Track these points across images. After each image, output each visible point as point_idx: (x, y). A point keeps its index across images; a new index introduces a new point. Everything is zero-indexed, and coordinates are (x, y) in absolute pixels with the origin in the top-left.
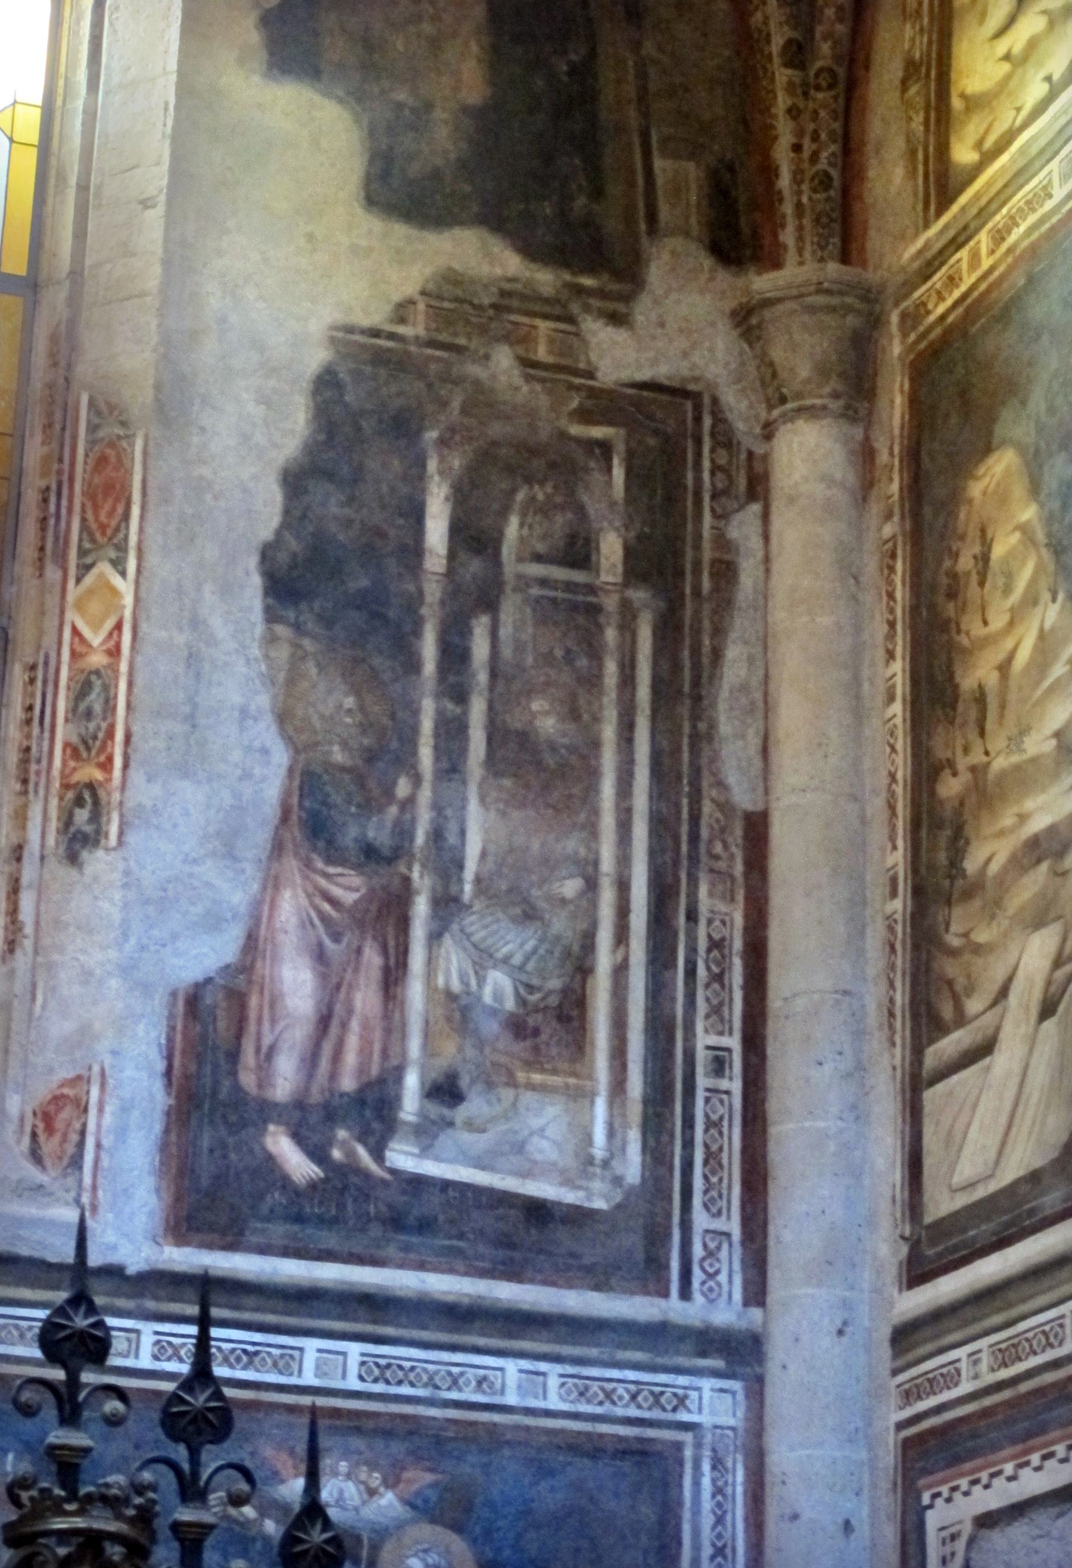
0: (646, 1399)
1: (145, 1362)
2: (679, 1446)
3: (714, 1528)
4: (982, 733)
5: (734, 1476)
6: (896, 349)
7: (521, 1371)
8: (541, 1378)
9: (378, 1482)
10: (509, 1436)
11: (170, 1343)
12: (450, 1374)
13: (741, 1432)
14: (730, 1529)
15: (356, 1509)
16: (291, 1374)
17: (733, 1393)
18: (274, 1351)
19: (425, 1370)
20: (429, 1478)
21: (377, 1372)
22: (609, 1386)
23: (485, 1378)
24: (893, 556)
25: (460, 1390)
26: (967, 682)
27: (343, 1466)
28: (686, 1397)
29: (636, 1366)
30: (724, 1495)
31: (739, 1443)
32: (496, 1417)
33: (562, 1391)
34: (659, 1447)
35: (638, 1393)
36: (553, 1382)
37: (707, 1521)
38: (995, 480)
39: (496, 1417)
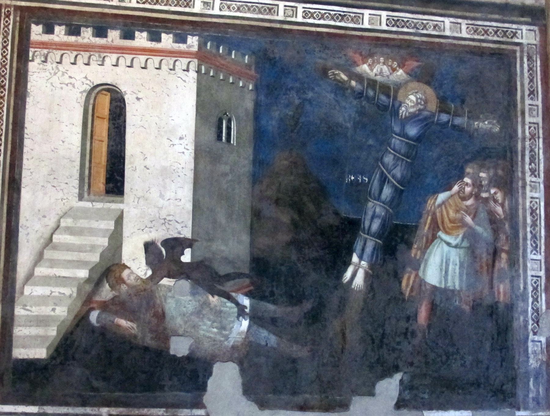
0: (501, 33)
1: (300, 19)
2: (515, 52)
3: (529, 84)
5: (536, 63)
7: (451, 22)
8: (459, 25)
9: (396, 66)
10: (447, 48)
11: (309, 12)
12: (423, 23)
13: (538, 46)
14: (535, 83)
15: (388, 76)
16: (359, 24)
17: (535, 31)
18: (351, 15)
19: (413, 22)
20: (416, 64)
21: (393, 23)
22: (486, 28)
23: (437, 25)
25: (427, 30)
27: (382, 59)
28: (516, 33)
29: (496, 21)
30: (533, 71)
31: (538, 50)
32: (442, 40)
33: (468, 30)
34: (506, 52)
35: (498, 30)
36: (464, 27)
37: (526, 81)
39: (442, 40)
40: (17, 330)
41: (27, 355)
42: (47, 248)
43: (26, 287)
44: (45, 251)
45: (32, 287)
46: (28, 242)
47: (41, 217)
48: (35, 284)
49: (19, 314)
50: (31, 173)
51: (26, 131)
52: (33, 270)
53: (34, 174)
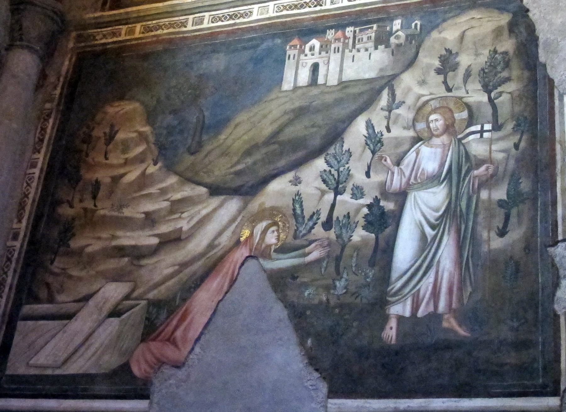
4: (94, 197)
6: (71, 45)
24: (49, 116)
26: (89, 176)
38: (124, 110)
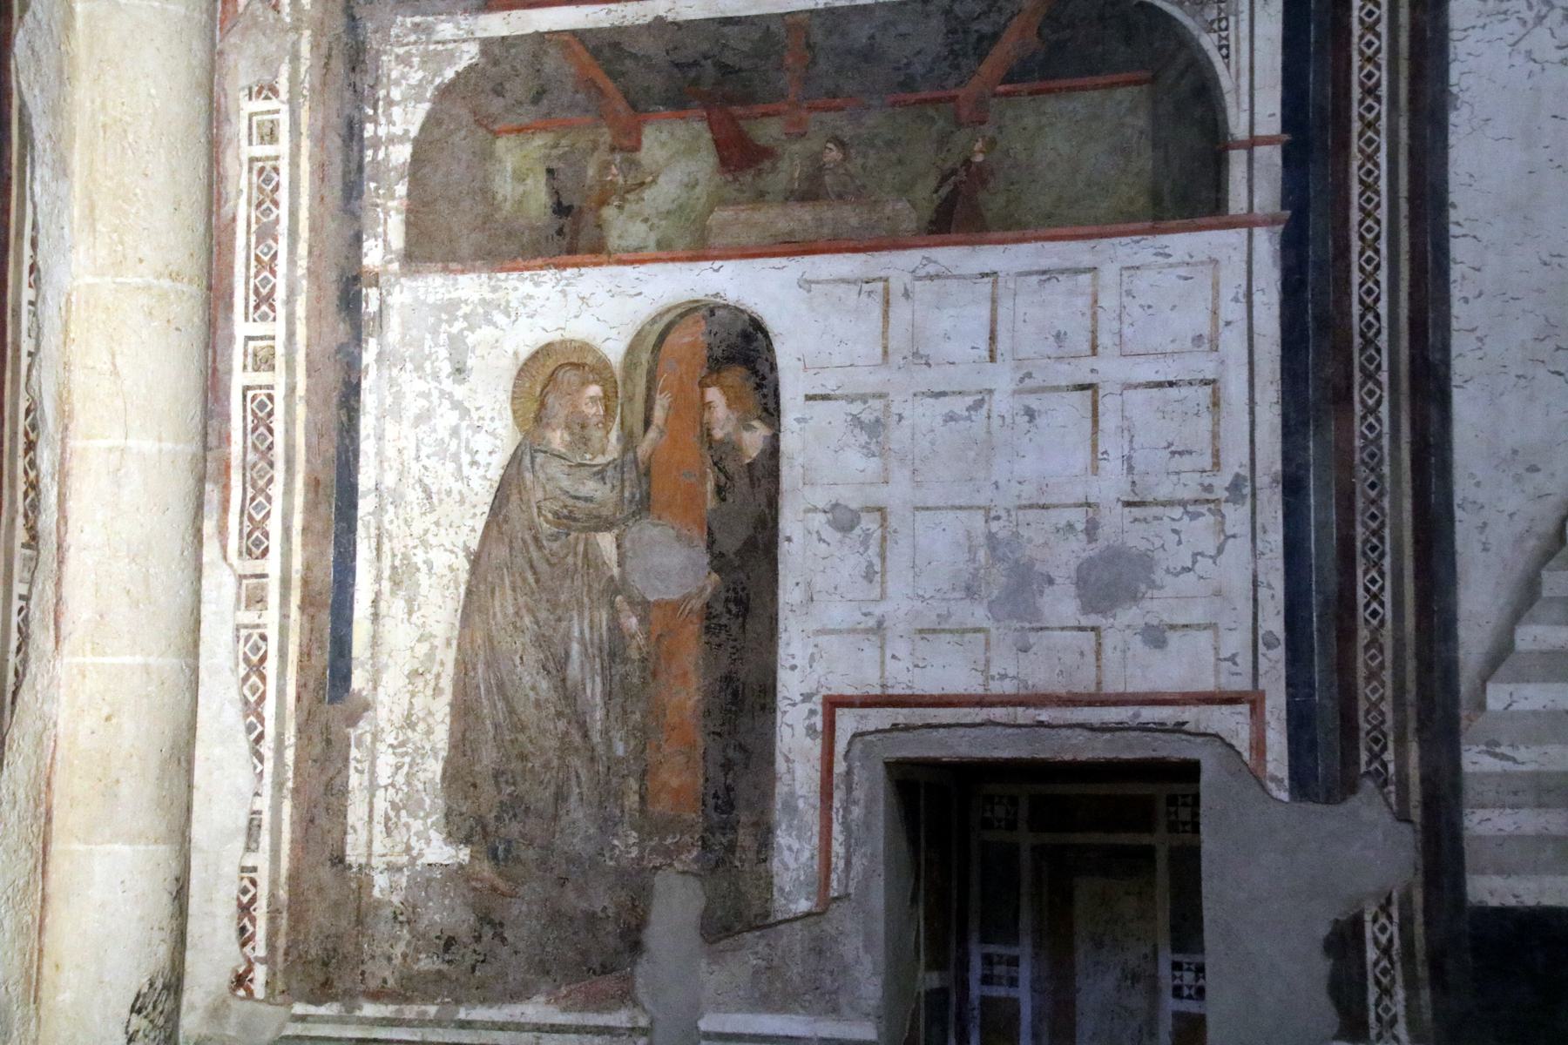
40: (1476, 818)
41: (1516, 896)
42: (1552, 563)
43: (1490, 687)
44: (1545, 574)
45: (1511, 687)
46: (1485, 550)
47: (1521, 470)
48: (1520, 677)
49: (1477, 768)
50: (1480, 339)
51: (1453, 215)
52: (1511, 632)
53: (1487, 341)
